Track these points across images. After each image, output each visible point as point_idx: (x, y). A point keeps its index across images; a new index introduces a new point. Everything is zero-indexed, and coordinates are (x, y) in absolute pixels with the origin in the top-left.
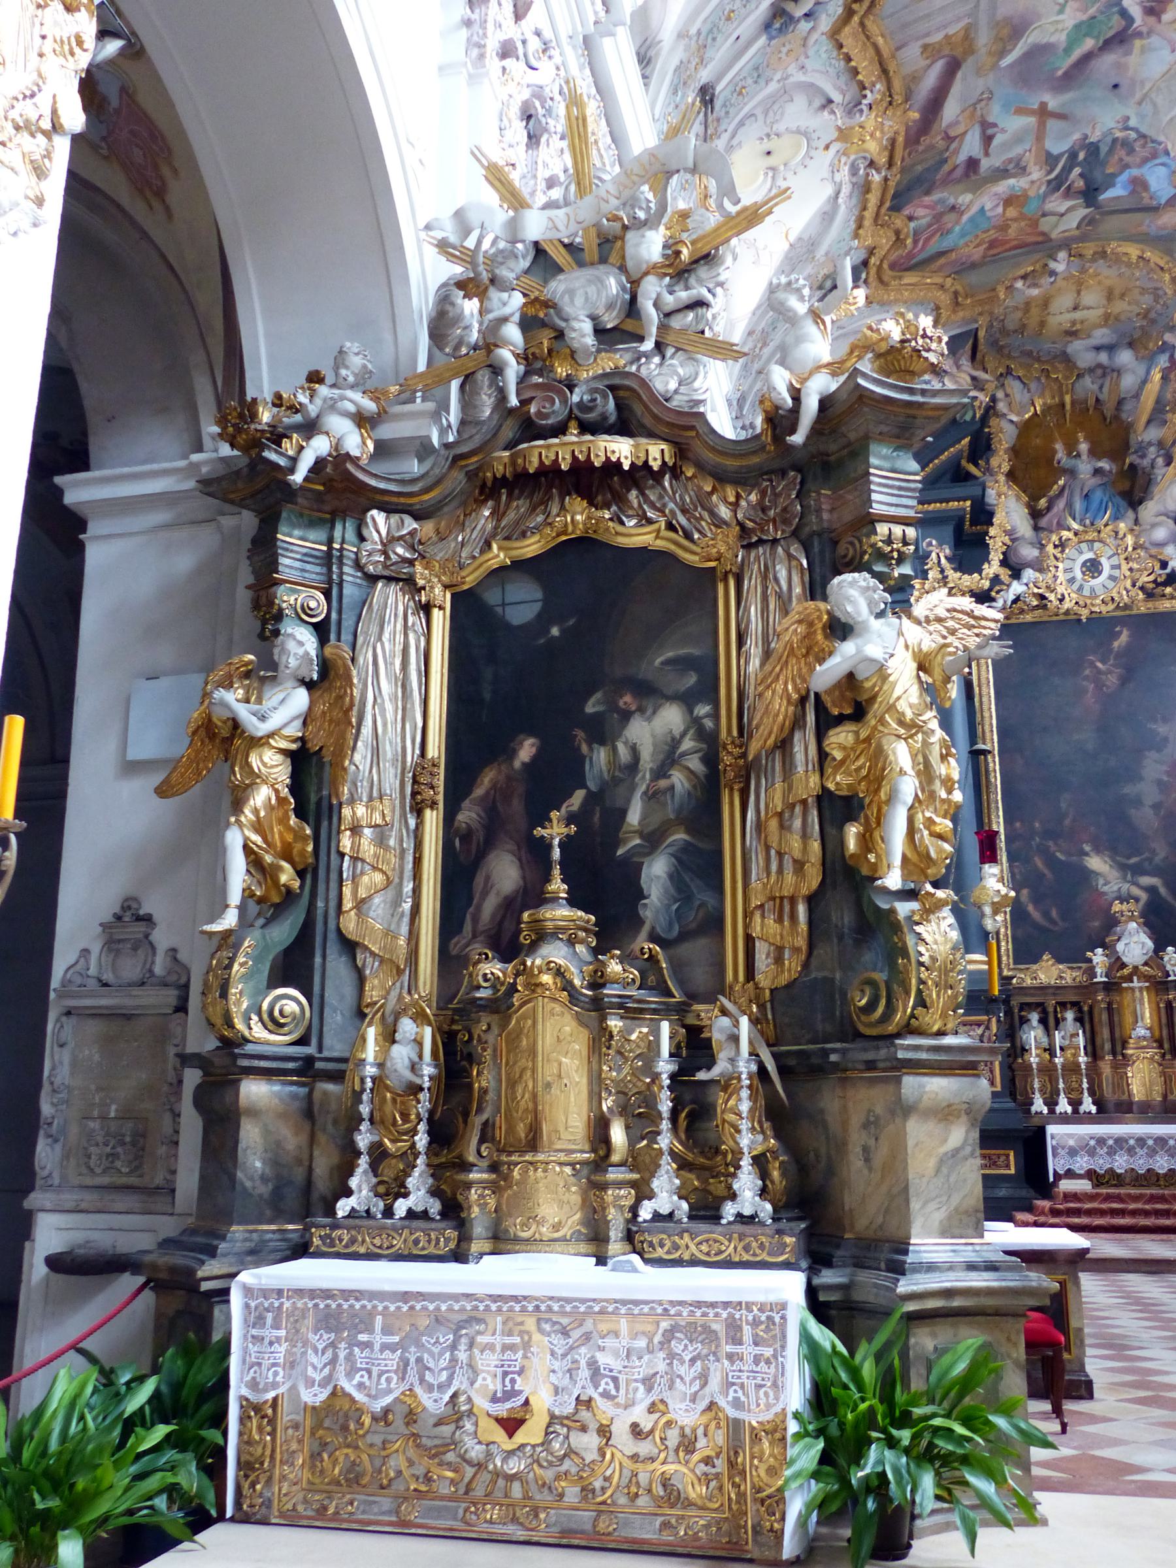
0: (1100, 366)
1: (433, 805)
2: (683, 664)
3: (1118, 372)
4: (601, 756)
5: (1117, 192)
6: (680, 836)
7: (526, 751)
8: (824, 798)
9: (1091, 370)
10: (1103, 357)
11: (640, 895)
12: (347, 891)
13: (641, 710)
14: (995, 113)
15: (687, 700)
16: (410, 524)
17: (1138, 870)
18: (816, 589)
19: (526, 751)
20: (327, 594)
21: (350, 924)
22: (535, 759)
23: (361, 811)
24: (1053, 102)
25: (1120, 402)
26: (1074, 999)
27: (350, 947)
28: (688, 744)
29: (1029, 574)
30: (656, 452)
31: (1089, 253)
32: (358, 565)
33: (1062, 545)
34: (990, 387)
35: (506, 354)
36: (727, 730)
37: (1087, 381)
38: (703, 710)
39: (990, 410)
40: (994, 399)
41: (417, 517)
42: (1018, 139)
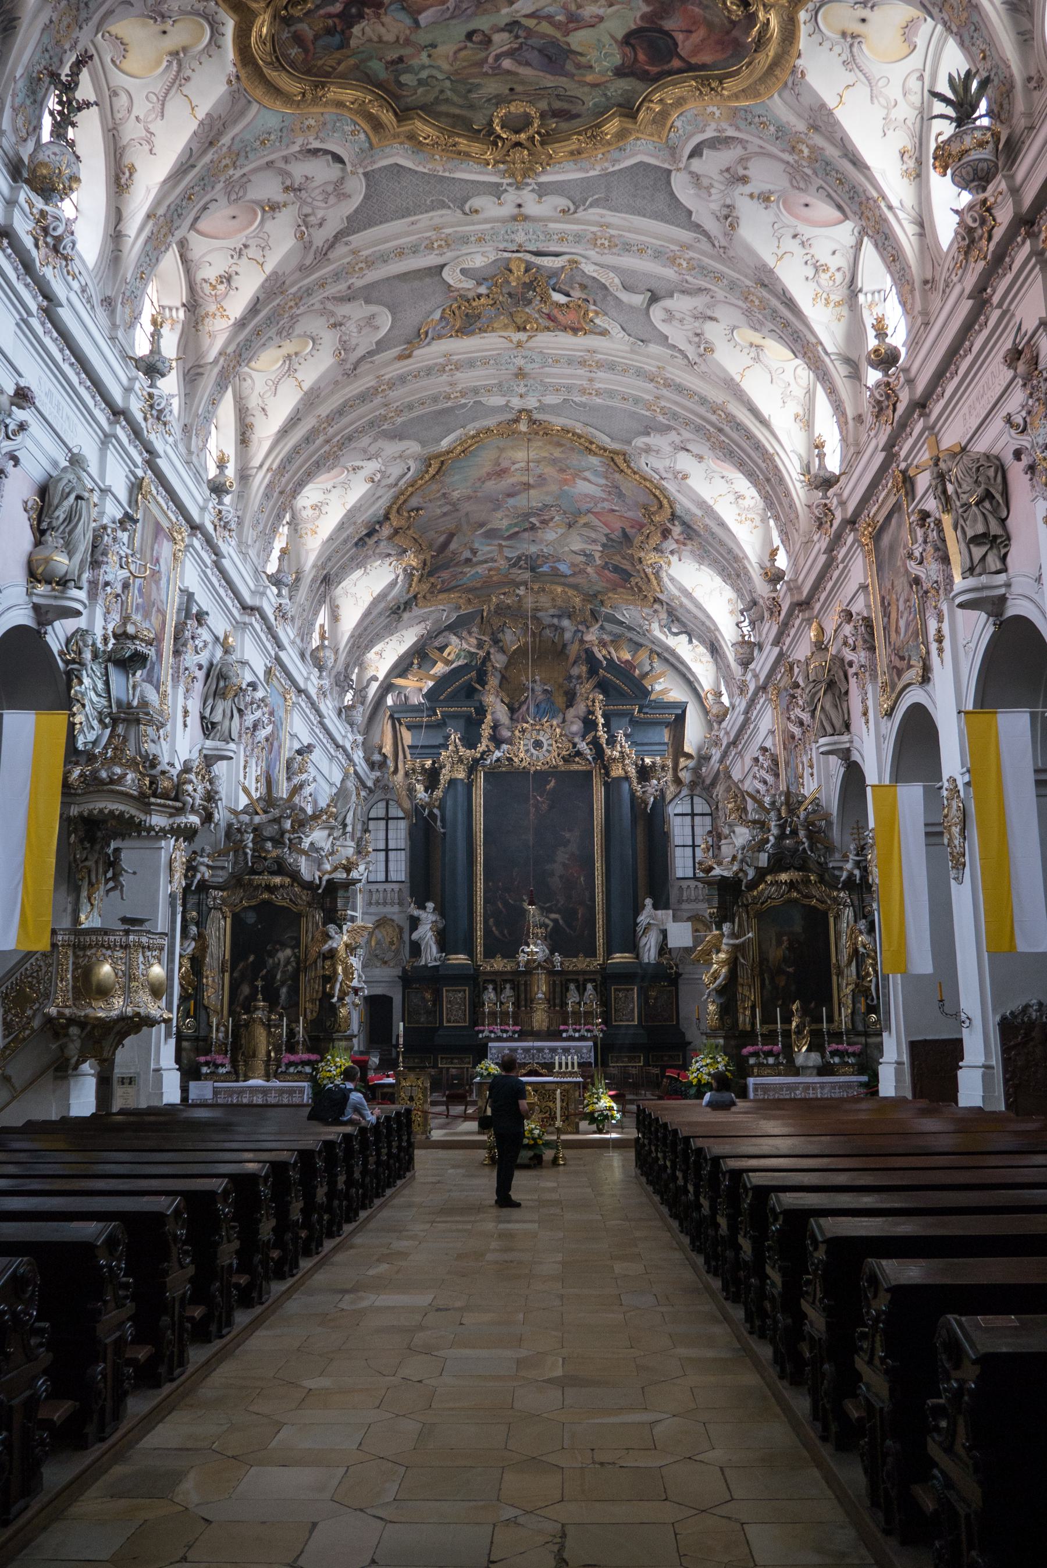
0: (553, 625)
2: (291, 938)
3: (563, 630)
5: (545, 569)
7: (252, 958)
8: (324, 976)
9: (550, 626)
10: (555, 621)
11: (279, 996)
14: (476, 545)
15: (293, 948)
17: (550, 910)
18: (325, 924)
19: (252, 958)
21: (206, 1002)
24: (504, 543)
25: (565, 646)
26: (509, 977)
27: (206, 1008)
29: (505, 747)
30: (288, 880)
31: (536, 587)
33: (523, 731)
34: (486, 647)
36: (302, 956)
37: (548, 631)
39: (487, 658)
40: (488, 653)
41: (222, 890)
42: (490, 552)
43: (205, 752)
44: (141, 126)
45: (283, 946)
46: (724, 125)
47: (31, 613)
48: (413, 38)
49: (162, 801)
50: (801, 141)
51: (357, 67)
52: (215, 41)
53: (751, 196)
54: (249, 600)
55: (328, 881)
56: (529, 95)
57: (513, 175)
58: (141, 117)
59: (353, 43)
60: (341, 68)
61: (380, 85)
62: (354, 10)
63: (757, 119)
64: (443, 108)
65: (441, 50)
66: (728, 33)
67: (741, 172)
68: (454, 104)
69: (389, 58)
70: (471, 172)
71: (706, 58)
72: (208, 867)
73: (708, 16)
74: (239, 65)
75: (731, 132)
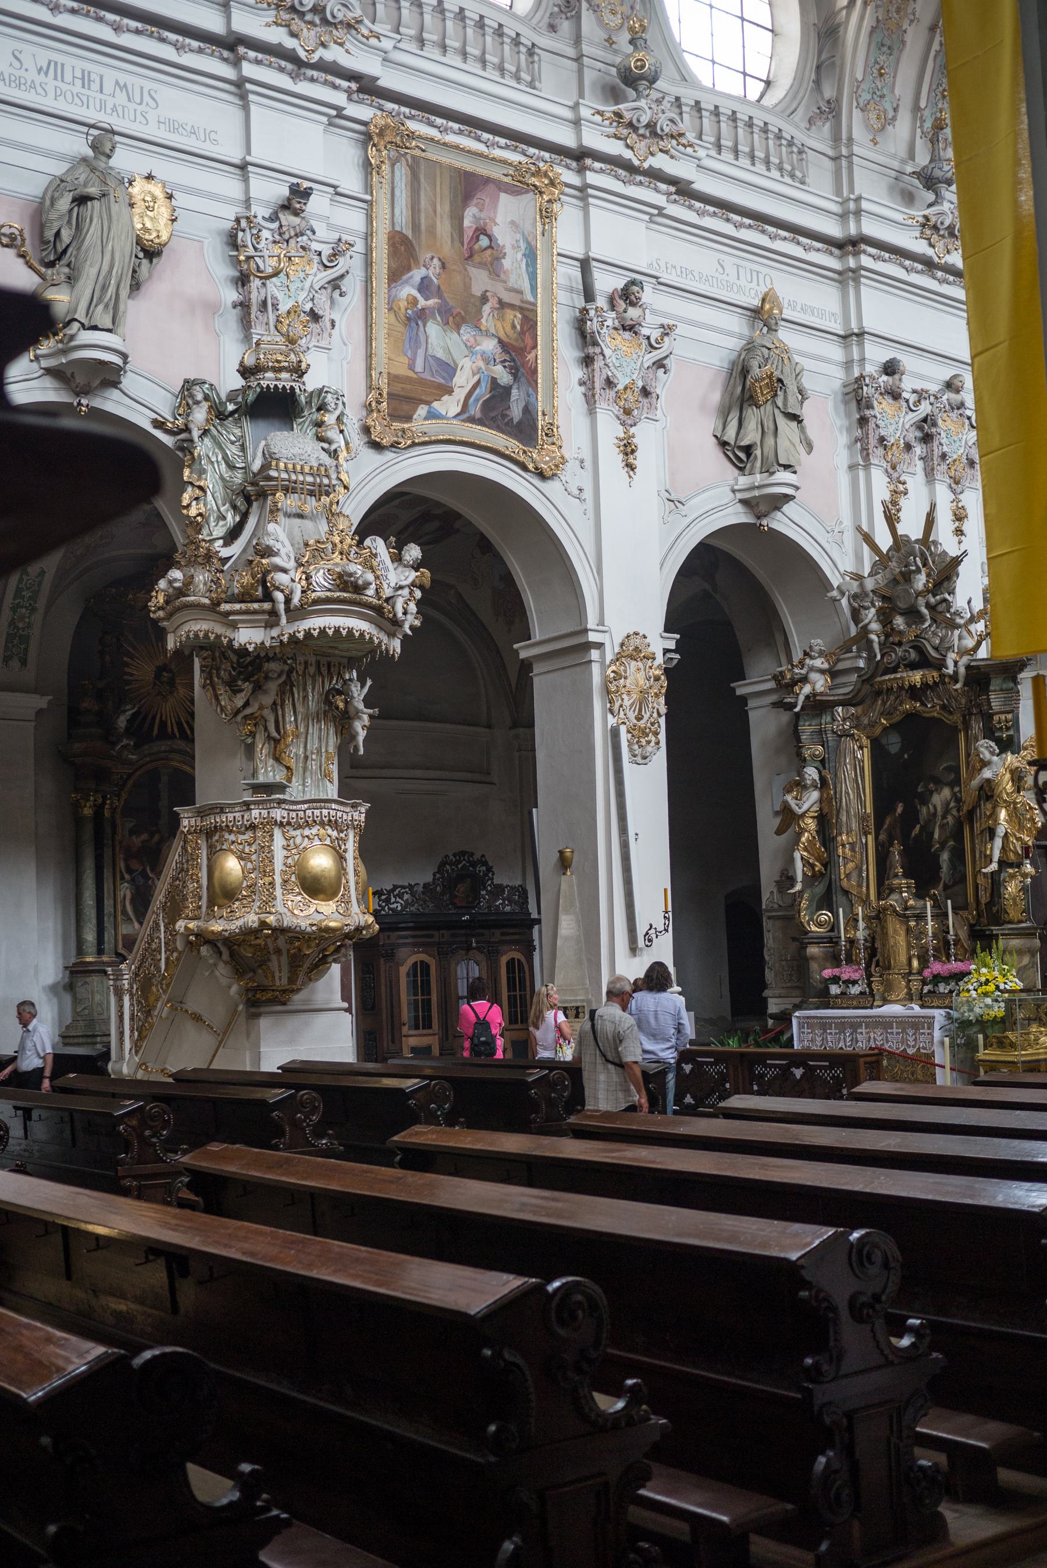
1: (870, 833)
4: (924, 810)
6: (951, 843)
7: (900, 809)
11: (940, 868)
12: (842, 871)
13: (936, 790)
16: (853, 710)
19: (900, 809)
20: (823, 746)
21: (845, 884)
22: (903, 811)
23: (844, 837)
27: (846, 893)
28: (952, 804)
32: (834, 732)
35: (874, 637)
38: (957, 789)
41: (853, 705)
43: (739, 496)
45: (939, 783)
47: (48, 382)
49: (243, 606)
54: (832, 229)
55: (968, 667)
72: (822, 672)
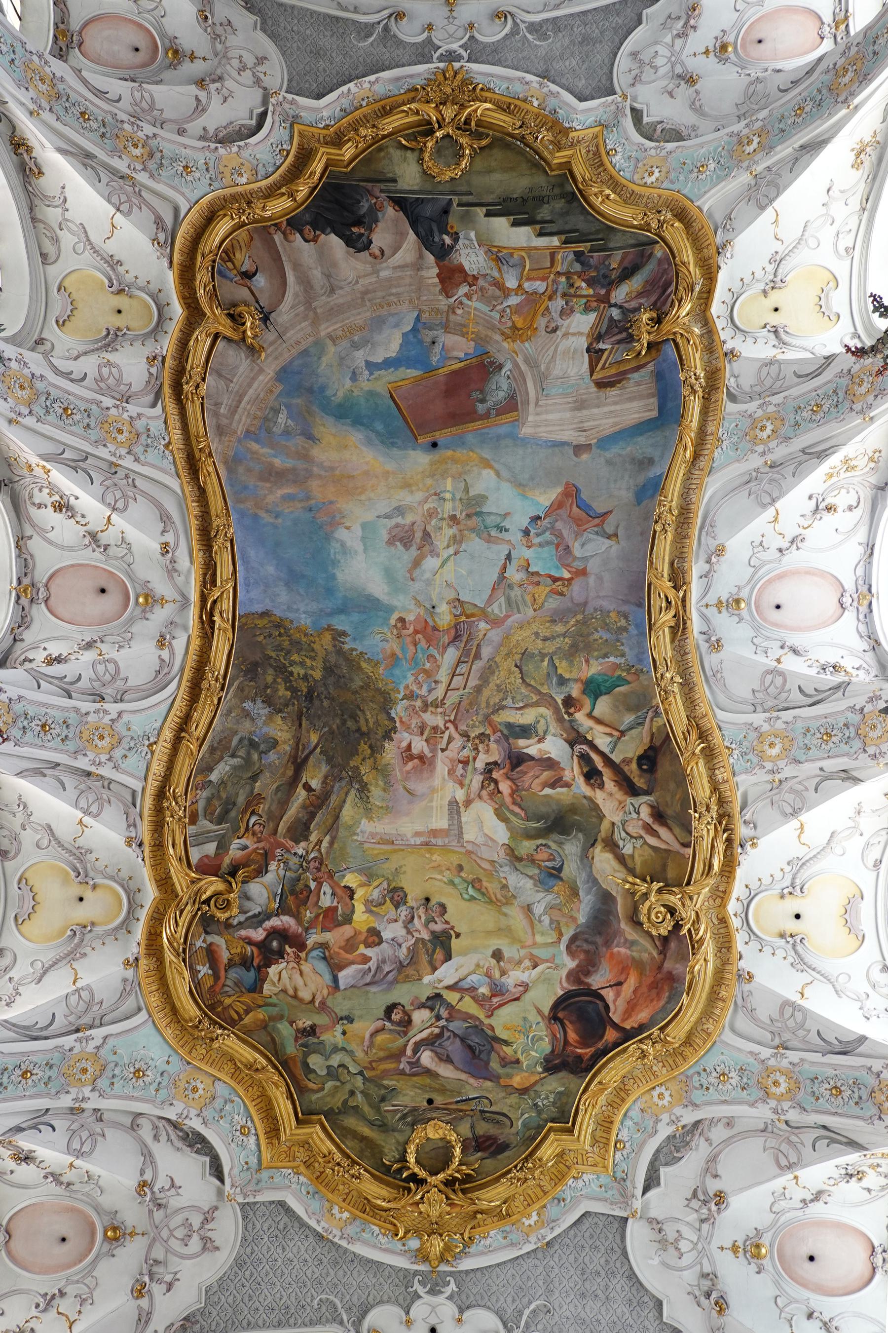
44: (11, 986)
46: (678, 1111)
48: (329, 1003)
50: (769, 1071)
51: (264, 1026)
52: (126, 926)
53: (735, 1249)
56: (451, 1111)
57: (426, 1259)
58: (16, 979)
59: (267, 988)
60: (247, 1020)
61: (285, 1064)
62: (275, 944)
63: (714, 1074)
64: (351, 1122)
65: (357, 1026)
66: (660, 968)
67: (713, 1186)
68: (364, 1118)
69: (300, 1024)
70: (374, 1246)
71: (643, 1016)
73: (634, 954)
74: (143, 946)
75: (689, 1117)
